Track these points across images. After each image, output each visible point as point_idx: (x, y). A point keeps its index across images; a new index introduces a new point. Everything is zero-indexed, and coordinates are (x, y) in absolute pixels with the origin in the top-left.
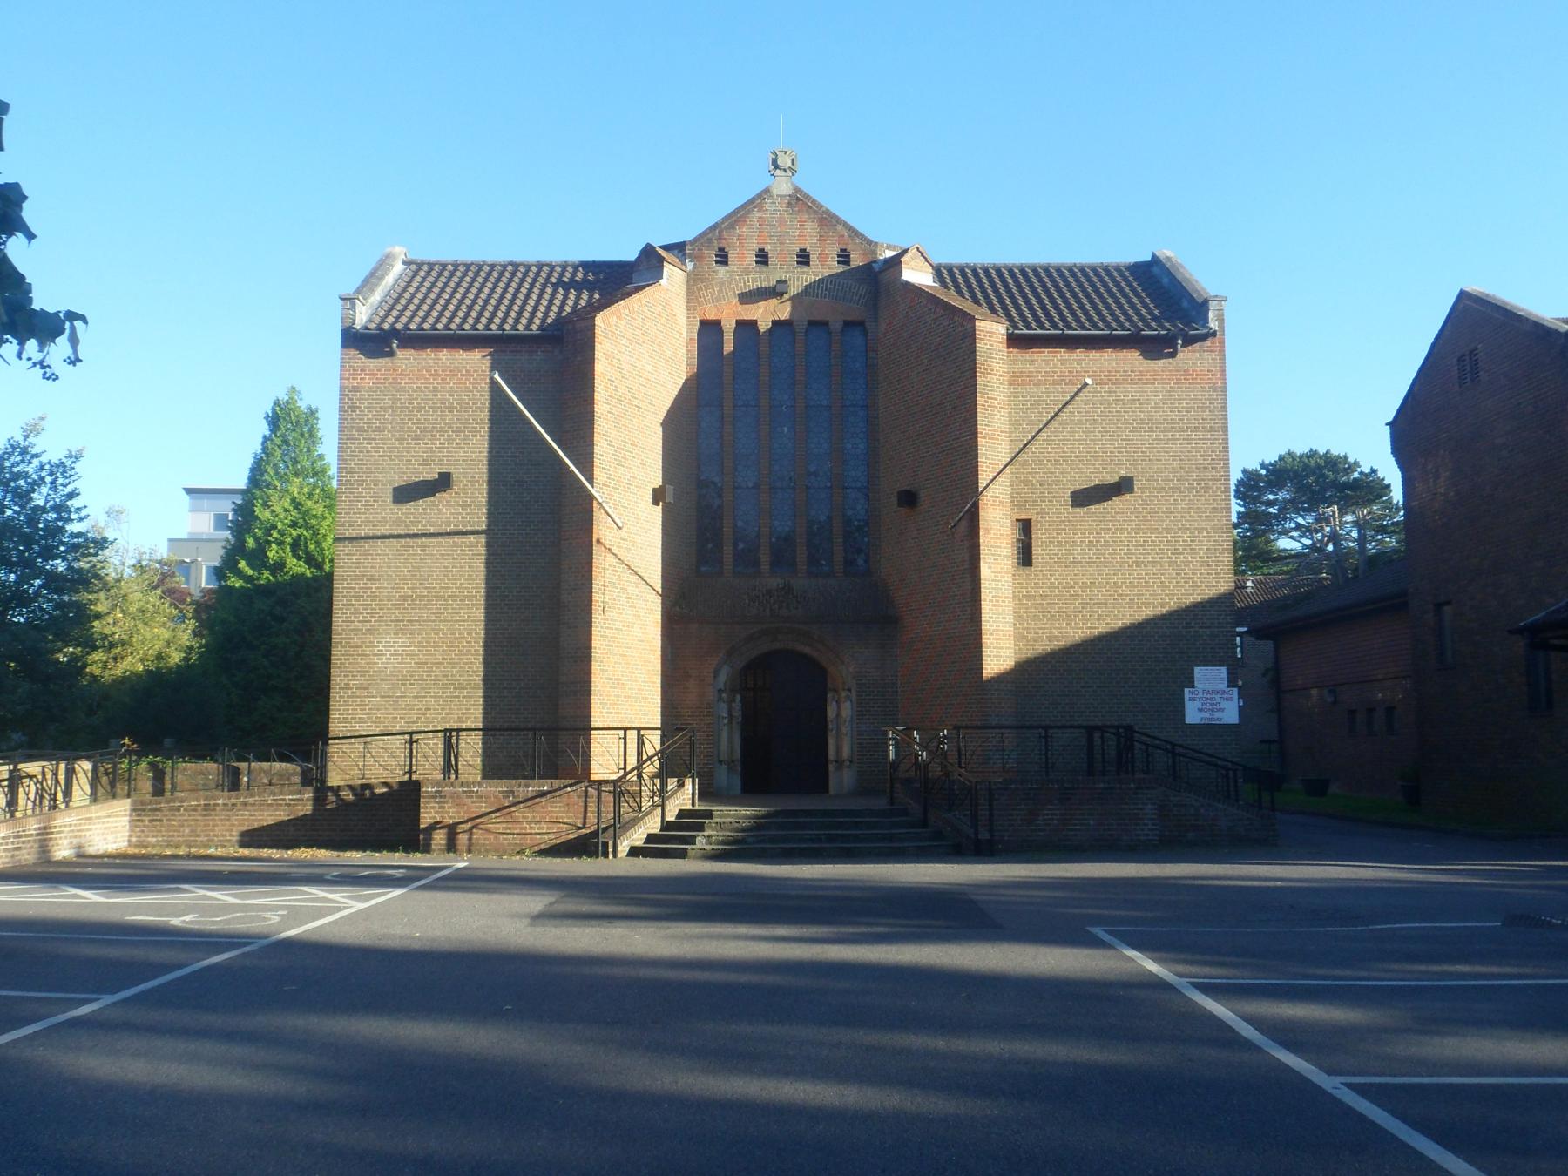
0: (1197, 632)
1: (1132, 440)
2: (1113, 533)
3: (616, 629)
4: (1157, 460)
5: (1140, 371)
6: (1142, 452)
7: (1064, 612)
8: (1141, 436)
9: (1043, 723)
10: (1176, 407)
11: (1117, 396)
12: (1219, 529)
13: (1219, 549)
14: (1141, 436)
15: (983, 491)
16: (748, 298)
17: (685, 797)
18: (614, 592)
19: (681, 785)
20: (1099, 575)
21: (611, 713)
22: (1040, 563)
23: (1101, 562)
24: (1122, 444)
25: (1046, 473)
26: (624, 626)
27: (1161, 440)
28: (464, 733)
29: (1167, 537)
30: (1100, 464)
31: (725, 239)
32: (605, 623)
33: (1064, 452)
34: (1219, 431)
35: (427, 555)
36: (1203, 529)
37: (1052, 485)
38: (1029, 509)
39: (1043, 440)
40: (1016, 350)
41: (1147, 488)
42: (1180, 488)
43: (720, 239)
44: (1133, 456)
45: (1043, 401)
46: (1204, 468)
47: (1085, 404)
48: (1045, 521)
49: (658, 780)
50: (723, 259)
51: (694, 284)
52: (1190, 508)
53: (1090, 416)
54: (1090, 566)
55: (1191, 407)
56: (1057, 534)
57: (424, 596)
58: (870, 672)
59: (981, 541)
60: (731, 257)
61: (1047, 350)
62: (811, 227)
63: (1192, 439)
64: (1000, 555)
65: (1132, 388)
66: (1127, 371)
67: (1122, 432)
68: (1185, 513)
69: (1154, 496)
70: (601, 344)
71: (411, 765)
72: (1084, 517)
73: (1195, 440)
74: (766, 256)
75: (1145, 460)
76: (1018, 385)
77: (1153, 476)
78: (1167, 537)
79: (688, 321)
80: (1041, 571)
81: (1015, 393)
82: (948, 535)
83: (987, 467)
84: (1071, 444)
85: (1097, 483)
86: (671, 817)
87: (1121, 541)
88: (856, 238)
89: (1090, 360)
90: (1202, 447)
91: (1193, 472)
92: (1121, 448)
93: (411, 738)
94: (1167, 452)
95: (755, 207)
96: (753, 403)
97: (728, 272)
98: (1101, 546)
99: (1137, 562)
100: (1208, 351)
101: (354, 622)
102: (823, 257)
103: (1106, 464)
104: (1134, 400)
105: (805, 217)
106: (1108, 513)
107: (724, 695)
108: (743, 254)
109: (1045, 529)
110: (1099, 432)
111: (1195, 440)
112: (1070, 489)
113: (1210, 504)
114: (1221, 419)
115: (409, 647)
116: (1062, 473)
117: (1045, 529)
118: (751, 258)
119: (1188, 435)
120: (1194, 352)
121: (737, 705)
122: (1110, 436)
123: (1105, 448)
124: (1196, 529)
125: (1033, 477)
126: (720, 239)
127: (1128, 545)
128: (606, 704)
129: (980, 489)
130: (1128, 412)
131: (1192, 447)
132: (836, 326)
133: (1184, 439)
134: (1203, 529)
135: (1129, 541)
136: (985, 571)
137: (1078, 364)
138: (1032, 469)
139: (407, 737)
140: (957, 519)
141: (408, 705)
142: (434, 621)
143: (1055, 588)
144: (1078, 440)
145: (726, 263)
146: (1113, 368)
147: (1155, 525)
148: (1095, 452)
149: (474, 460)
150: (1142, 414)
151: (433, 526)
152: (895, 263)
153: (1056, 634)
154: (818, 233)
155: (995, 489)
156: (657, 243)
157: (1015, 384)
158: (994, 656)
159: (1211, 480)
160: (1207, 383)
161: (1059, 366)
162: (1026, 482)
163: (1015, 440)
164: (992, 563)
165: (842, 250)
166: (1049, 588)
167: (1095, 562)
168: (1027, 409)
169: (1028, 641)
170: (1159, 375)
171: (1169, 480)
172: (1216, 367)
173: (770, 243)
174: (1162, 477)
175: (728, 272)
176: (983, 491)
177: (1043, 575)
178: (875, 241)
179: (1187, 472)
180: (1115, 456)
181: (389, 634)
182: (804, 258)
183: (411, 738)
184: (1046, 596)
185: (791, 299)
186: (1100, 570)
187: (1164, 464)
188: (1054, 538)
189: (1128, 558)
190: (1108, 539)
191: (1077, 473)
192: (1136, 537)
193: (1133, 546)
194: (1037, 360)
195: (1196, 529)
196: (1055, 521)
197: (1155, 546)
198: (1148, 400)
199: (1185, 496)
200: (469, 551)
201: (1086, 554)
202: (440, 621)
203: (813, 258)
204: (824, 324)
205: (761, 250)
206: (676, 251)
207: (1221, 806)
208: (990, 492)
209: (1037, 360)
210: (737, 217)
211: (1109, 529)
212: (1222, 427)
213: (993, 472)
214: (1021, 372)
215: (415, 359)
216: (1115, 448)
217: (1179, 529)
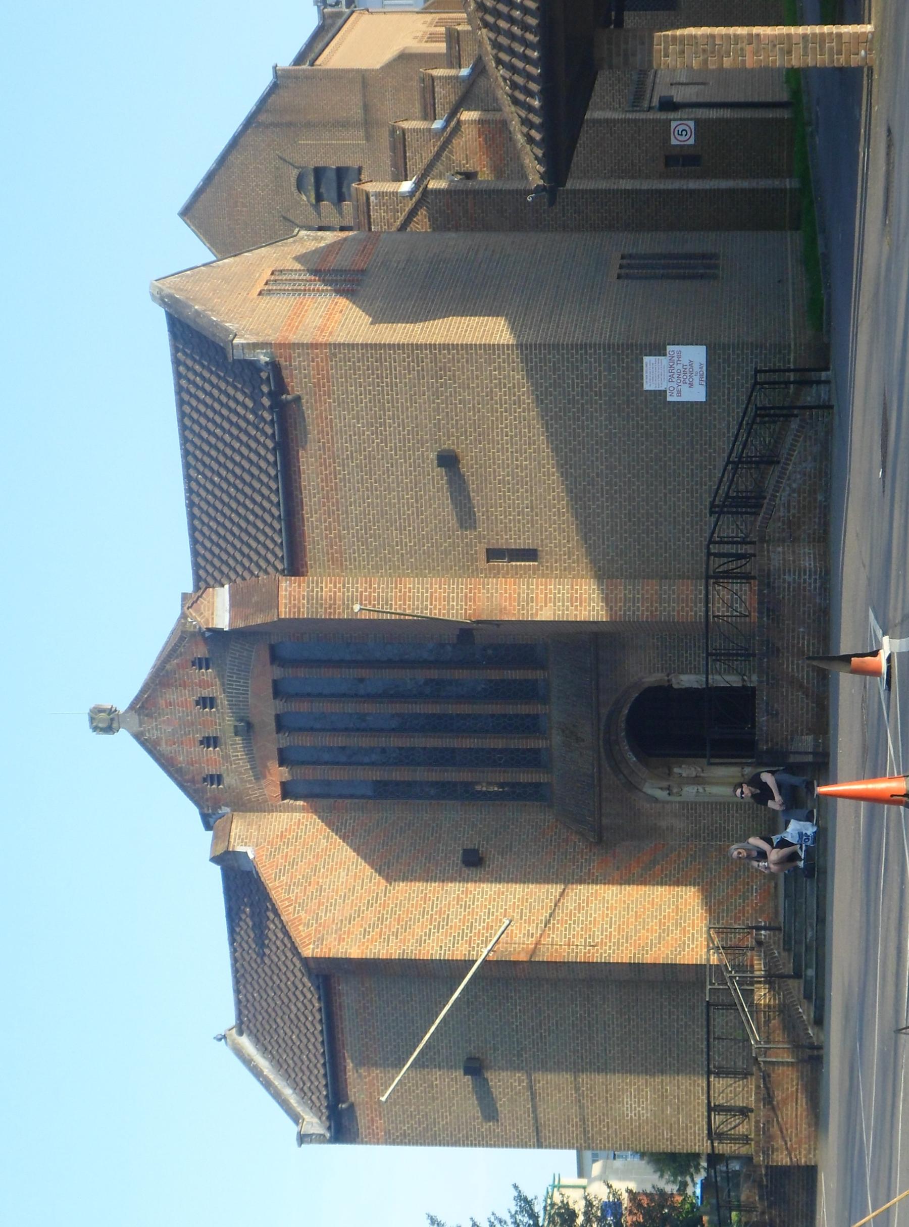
0: (605, 385)
1: (395, 444)
4: (416, 419)
5: (318, 434)
8: (390, 435)
9: (704, 558)
10: (356, 397)
11: (348, 459)
12: (490, 358)
13: (513, 359)
14: (390, 435)
17: (772, 941)
20: (544, 483)
22: (533, 542)
23: (531, 481)
24: (400, 455)
25: (436, 533)
27: (393, 415)
29: (501, 412)
30: (424, 478)
31: (194, 777)
33: (413, 514)
36: (491, 374)
37: (449, 527)
38: (476, 551)
41: (448, 431)
42: (446, 397)
43: (193, 781)
44: (413, 444)
45: (357, 533)
46: (423, 370)
47: (359, 491)
48: (488, 534)
50: (216, 779)
51: (243, 805)
52: (469, 388)
53: (372, 486)
54: (536, 492)
55: (355, 381)
56: (501, 523)
58: (650, 661)
60: (213, 771)
62: (171, 695)
63: (391, 382)
65: (337, 443)
66: (319, 447)
67: (387, 455)
68: (473, 393)
69: (457, 424)
70: (330, 949)
72: (482, 496)
73: (391, 379)
74: (208, 738)
75: (417, 431)
76: (341, 557)
77: (435, 424)
78: (501, 412)
79: (285, 812)
80: (542, 540)
81: (350, 560)
87: (508, 460)
88: (178, 652)
89: (309, 483)
90: (400, 371)
92: (405, 456)
95: (155, 749)
97: (228, 775)
98: (513, 479)
99: (530, 444)
100: (290, 361)
102: (203, 684)
103: (424, 472)
104: (351, 440)
106: (477, 471)
108: (208, 760)
110: (389, 478)
111: (391, 379)
113: (463, 366)
114: (367, 350)
116: (435, 517)
119: (387, 386)
120: (292, 375)
122: (392, 467)
123: (406, 471)
125: (441, 546)
126: (193, 781)
127: (512, 452)
130: (365, 448)
131: (401, 382)
133: (392, 390)
134: (491, 374)
135: (507, 452)
136: (546, 614)
137: (315, 497)
138: (432, 546)
141: (686, 1094)
143: (559, 528)
144: (399, 501)
146: (316, 461)
147: (488, 424)
148: (411, 482)
150: (367, 433)
154: (177, 688)
159: (436, 364)
160: (327, 364)
161: (318, 515)
162: (446, 553)
163: (403, 562)
166: (560, 534)
167: (531, 487)
168: (367, 549)
170: (321, 413)
171: (439, 408)
172: (308, 354)
174: (435, 416)
175: (228, 775)
177: (546, 539)
179: (428, 388)
180: (415, 462)
181: (619, 1109)
182: (207, 702)
184: (569, 536)
186: (540, 481)
187: (421, 413)
188: (506, 527)
189: (525, 453)
190: (505, 473)
191: (435, 502)
192: (502, 444)
193: (512, 448)
196: (488, 526)
197: (511, 425)
198: (350, 427)
199: (455, 392)
201: (522, 496)
203: (206, 693)
205: (201, 743)
207: (790, 468)
209: (313, 538)
210: (168, 764)
211: (494, 471)
212: (376, 350)
215: (354, 1087)
216: (405, 462)
217: (492, 399)
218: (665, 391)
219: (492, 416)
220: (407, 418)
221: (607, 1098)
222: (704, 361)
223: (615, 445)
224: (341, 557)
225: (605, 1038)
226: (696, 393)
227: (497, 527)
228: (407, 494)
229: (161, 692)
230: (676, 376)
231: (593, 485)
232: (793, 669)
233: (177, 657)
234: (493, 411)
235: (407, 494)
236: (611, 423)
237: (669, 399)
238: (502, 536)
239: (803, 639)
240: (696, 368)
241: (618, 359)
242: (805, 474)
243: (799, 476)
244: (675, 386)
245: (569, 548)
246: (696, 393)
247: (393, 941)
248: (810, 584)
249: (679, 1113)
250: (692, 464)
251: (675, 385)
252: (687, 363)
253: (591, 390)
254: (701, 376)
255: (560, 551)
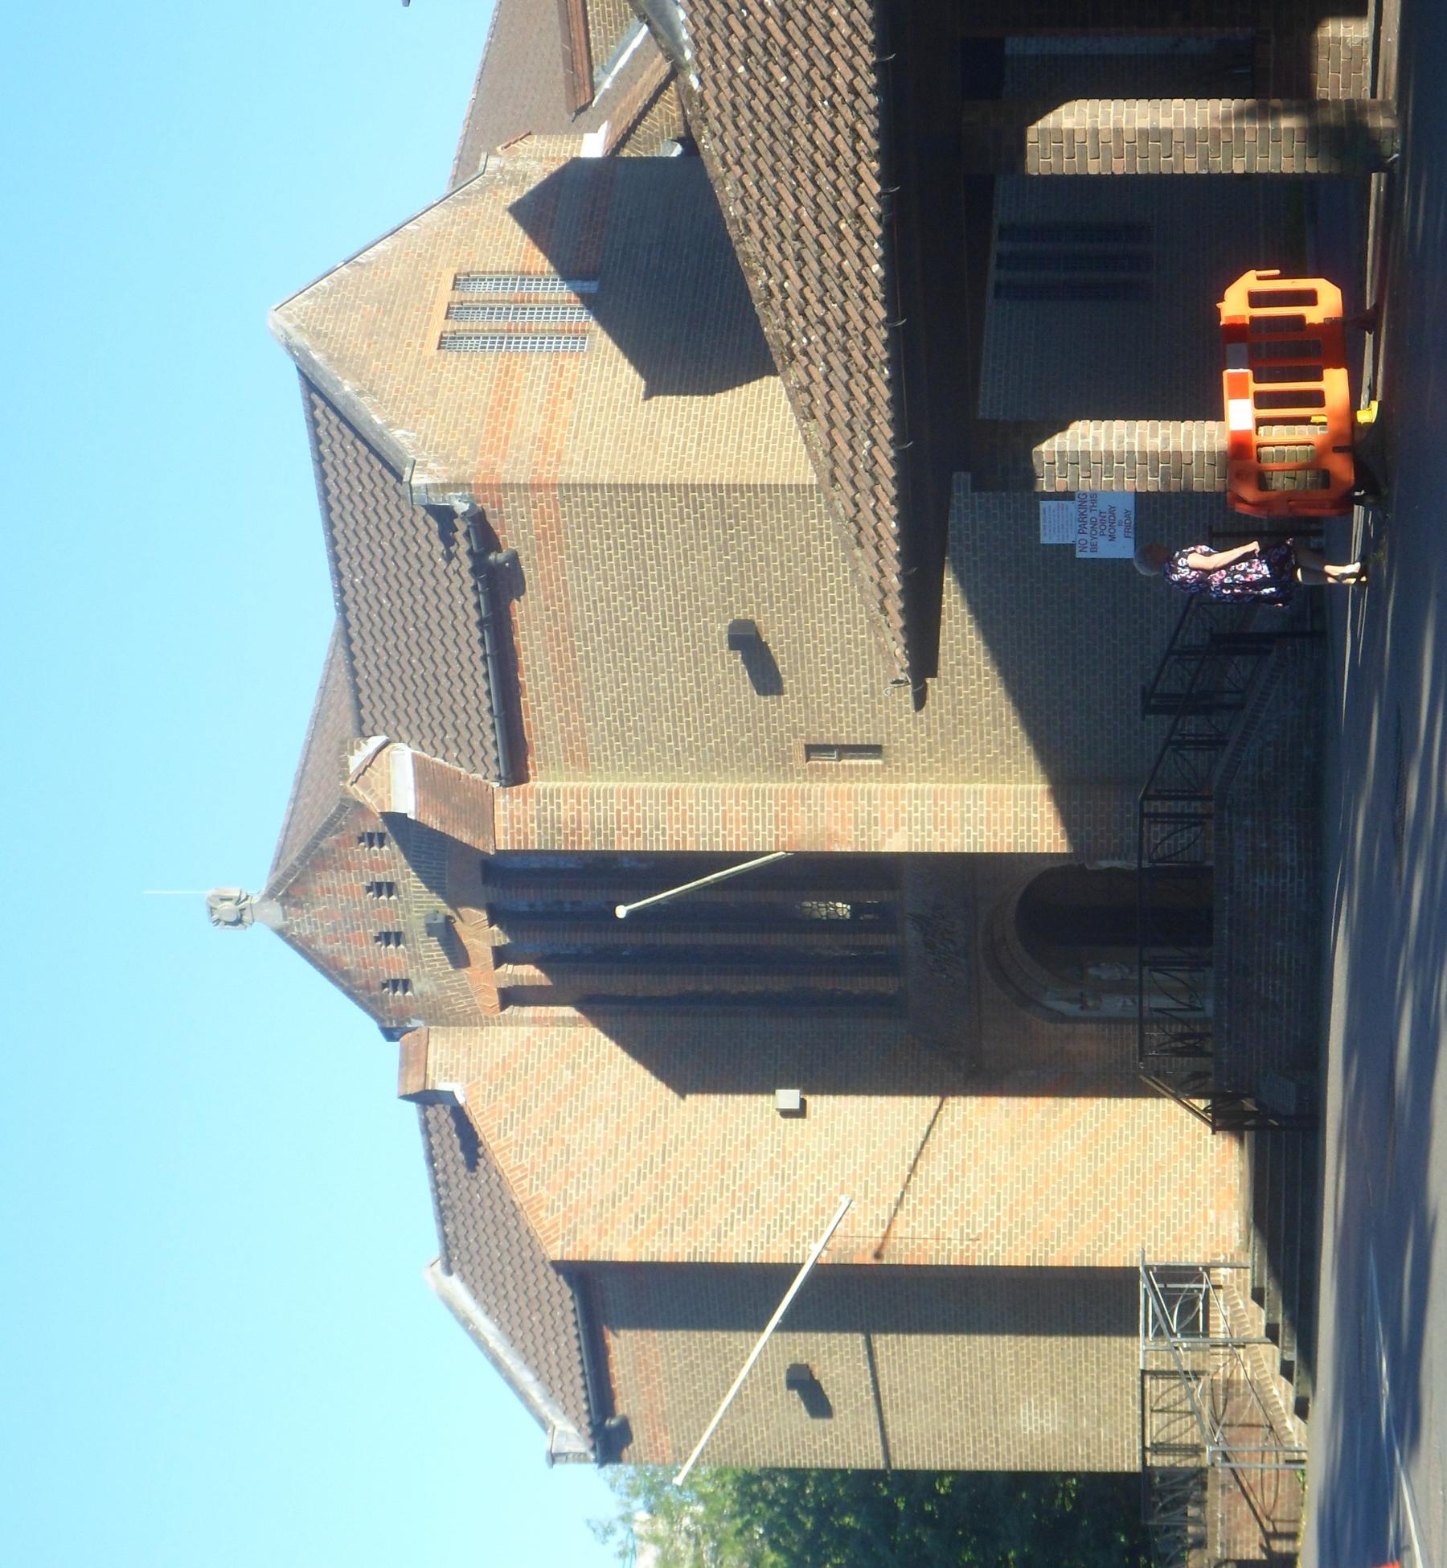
5: (546, 599)
6: (683, 600)
7: (954, 708)
11: (591, 631)
14: (655, 601)
16: (458, 955)
27: (659, 575)
34: (638, 497)
40: (530, 758)
60: (395, 975)
61: (524, 719)
62: (329, 879)
68: (781, 546)
80: (889, 734)
84: (678, 692)
85: (739, 660)
91: (711, 533)
94: (680, 567)
105: (315, 888)
109: (820, 727)
110: (654, 655)
112: (752, 696)
127: (841, 623)
154: (337, 871)
157: (586, 760)
167: (871, 668)
169: (1002, 753)
170: (549, 574)
173: (365, 930)
184: (929, 729)
185: (454, 906)
194: (542, 732)
203: (380, 877)
205: (377, 939)
210: (331, 969)
214: (565, 751)
217: (809, 555)
220: (681, 578)
227: (820, 717)
229: (314, 876)
233: (336, 832)
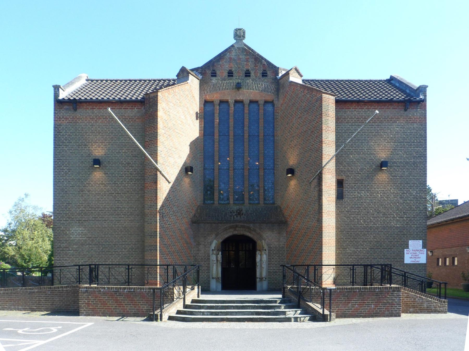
2: (378, 185)
3: (168, 224)
15: (325, 165)
18: (167, 209)
19: (193, 289)
21: (166, 258)
26: (172, 223)
28: (101, 266)
31: (215, 66)
32: (163, 222)
35: (90, 194)
39: (349, 146)
49: (182, 287)
51: (202, 84)
57: (90, 211)
59: (323, 187)
60: (218, 73)
64: (331, 194)
71: (79, 278)
82: (308, 186)
83: (326, 156)
86: (188, 302)
93: (79, 268)
96: (227, 134)
101: (62, 221)
107: (214, 252)
115: (83, 231)
117: (349, 184)
118: (226, 74)
121: (220, 256)
124: (412, 183)
128: (164, 255)
129: (323, 166)
132: (261, 103)
139: (77, 267)
140: (312, 179)
142: (94, 221)
145: (215, 76)
149: (109, 154)
151: (93, 182)
152: (287, 74)
153: (353, 227)
154: (254, 63)
155: (329, 166)
156: (189, 68)
158: (327, 236)
164: (327, 197)
165: (264, 71)
176: (325, 165)
177: (348, 203)
178: (278, 66)
183: (79, 268)
195: (412, 183)
200: (107, 192)
202: (96, 221)
203: (252, 74)
204: (257, 102)
205: (230, 71)
206: (195, 72)
208: (327, 167)
213: (328, 159)
218: (408, 248)
219: (398, 184)
221: (81, 221)
222: (420, 262)
223: (387, 230)
224: (339, 122)
225: (112, 221)
226: (408, 260)
228: (366, 150)
230: (414, 252)
231: (370, 221)
232: (352, 303)
234: (401, 184)
235: (366, 150)
236: (396, 228)
237: (405, 250)
238: (349, 185)
239: (368, 307)
240: (417, 260)
241: (421, 231)
242: (421, 303)
243: (421, 301)
244: (410, 252)
245: (344, 211)
246: (408, 260)
247: (163, 131)
248: (394, 309)
249: (74, 251)
250: (379, 259)
251: (411, 252)
252: (419, 256)
253: (409, 221)
254: (415, 262)
255: (343, 208)
